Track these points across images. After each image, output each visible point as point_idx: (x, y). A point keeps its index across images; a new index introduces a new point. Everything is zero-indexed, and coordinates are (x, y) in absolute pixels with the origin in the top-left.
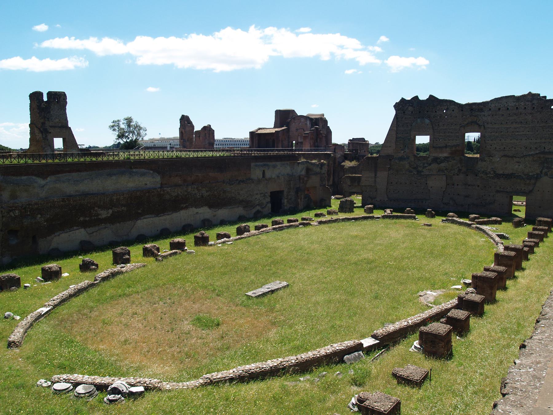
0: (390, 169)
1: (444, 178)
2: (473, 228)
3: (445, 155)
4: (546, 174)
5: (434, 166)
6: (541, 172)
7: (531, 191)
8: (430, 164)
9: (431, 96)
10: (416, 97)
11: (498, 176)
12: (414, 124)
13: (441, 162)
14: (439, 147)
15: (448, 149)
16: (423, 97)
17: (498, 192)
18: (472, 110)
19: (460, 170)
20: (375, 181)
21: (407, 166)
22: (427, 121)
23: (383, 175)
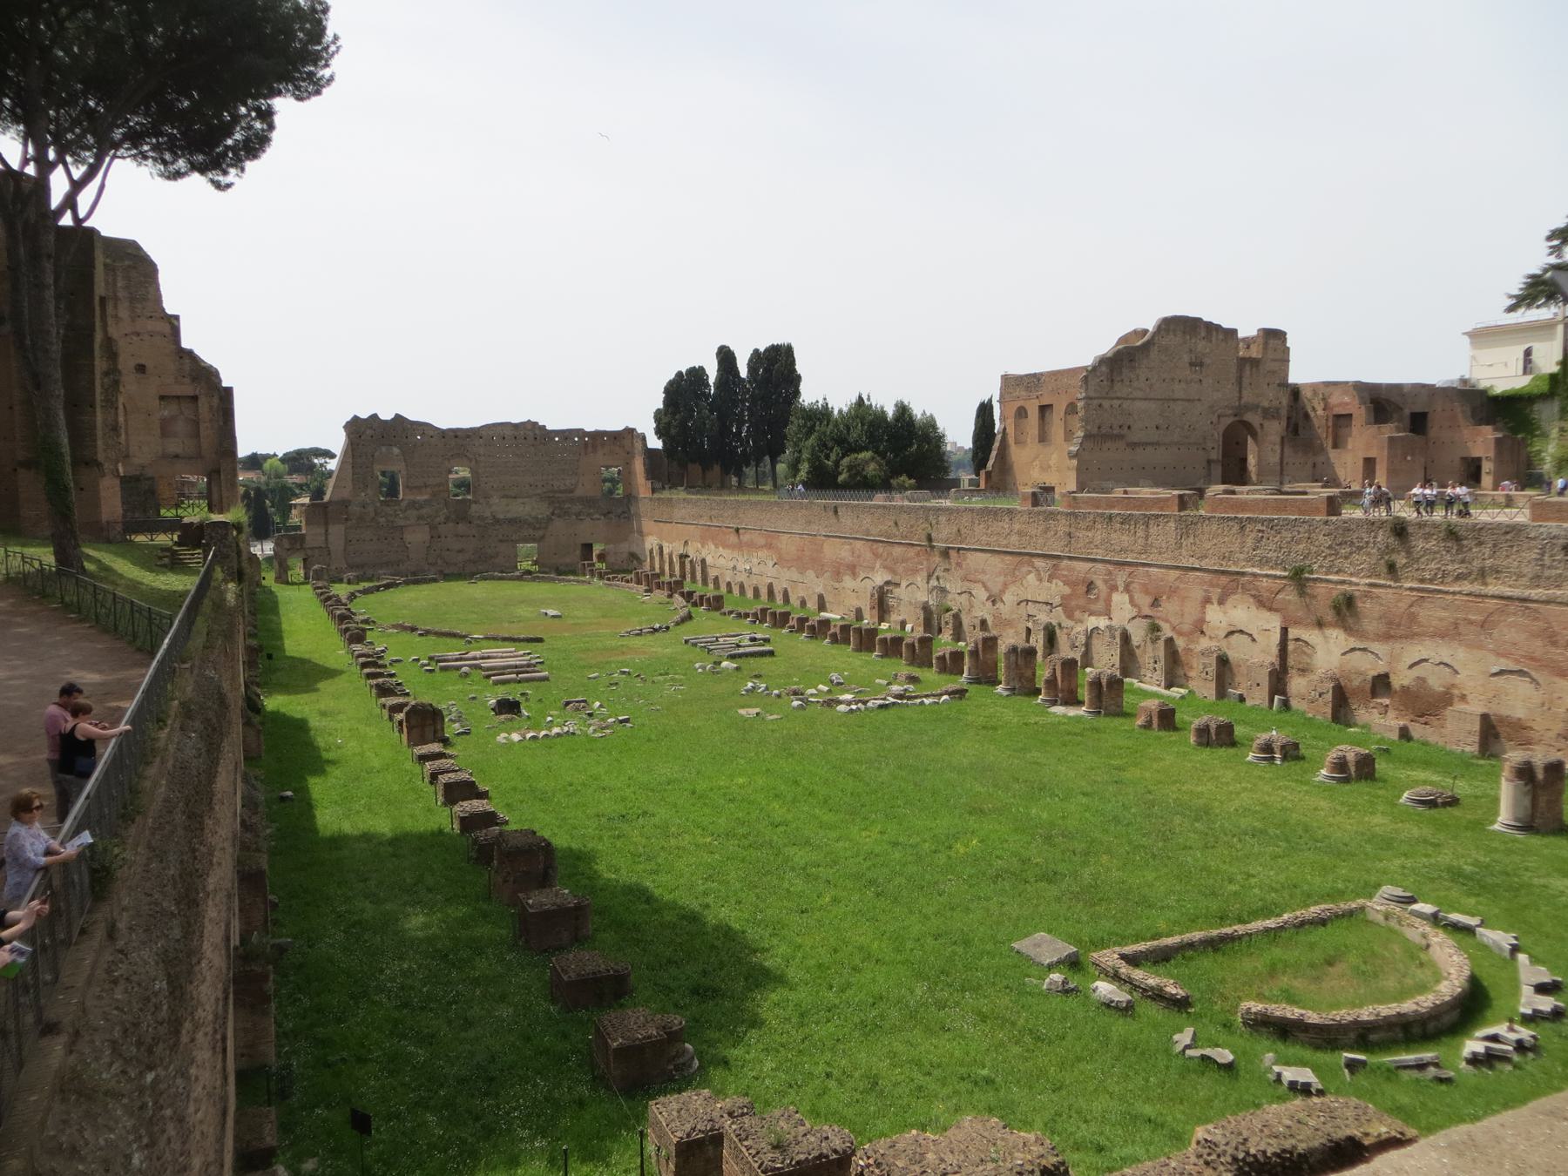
0: (346, 519)
1: (427, 528)
2: (525, 580)
3: (426, 497)
4: (559, 516)
5: (413, 513)
6: (553, 514)
7: (543, 537)
8: (405, 511)
9: (398, 417)
10: (374, 417)
11: (497, 521)
12: (377, 454)
13: (421, 507)
14: (416, 487)
15: (429, 489)
16: (386, 415)
17: (501, 541)
18: (456, 437)
19: (447, 519)
20: (326, 539)
21: (372, 514)
22: (396, 450)
23: (337, 531)
